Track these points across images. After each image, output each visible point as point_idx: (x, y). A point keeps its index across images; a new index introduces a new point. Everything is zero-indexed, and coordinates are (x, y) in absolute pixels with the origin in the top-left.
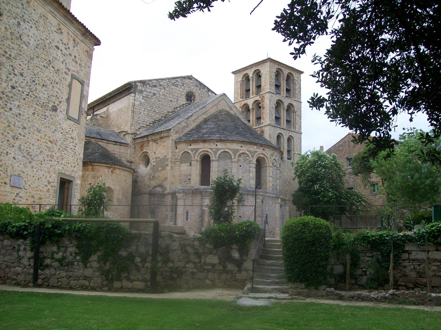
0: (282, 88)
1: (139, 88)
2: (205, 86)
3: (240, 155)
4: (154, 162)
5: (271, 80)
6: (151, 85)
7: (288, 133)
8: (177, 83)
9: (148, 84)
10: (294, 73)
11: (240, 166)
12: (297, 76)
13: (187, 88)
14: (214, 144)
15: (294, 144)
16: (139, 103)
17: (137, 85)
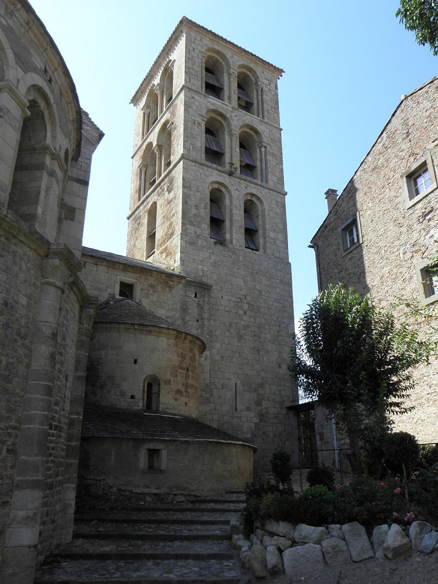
7: (243, 186)
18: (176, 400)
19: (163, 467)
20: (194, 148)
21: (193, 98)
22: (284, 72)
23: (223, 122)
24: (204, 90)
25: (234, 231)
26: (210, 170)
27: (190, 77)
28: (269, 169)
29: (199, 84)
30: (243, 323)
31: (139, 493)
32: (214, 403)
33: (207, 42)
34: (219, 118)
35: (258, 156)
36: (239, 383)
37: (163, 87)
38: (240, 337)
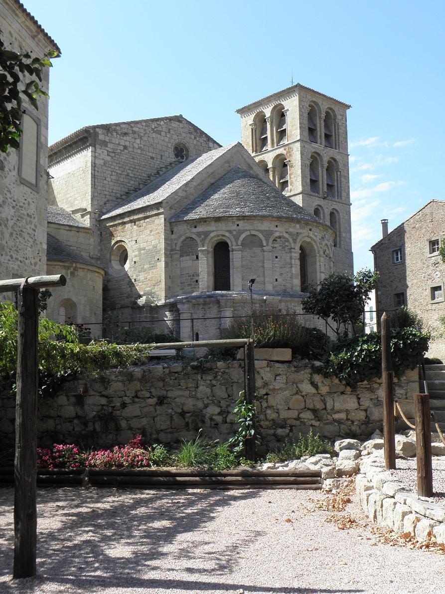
0: (319, 134)
1: (101, 137)
2: (202, 133)
3: (275, 240)
4: (136, 256)
5: (301, 121)
6: (119, 132)
8: (160, 129)
9: (115, 130)
10: (336, 108)
11: (276, 257)
12: (341, 113)
13: (175, 137)
14: (233, 223)
16: (101, 162)
17: (98, 133)
23: (318, 158)
26: (314, 197)
28: (342, 189)
29: (306, 133)
33: (309, 97)
34: (316, 156)
35: (336, 178)
37: (273, 118)
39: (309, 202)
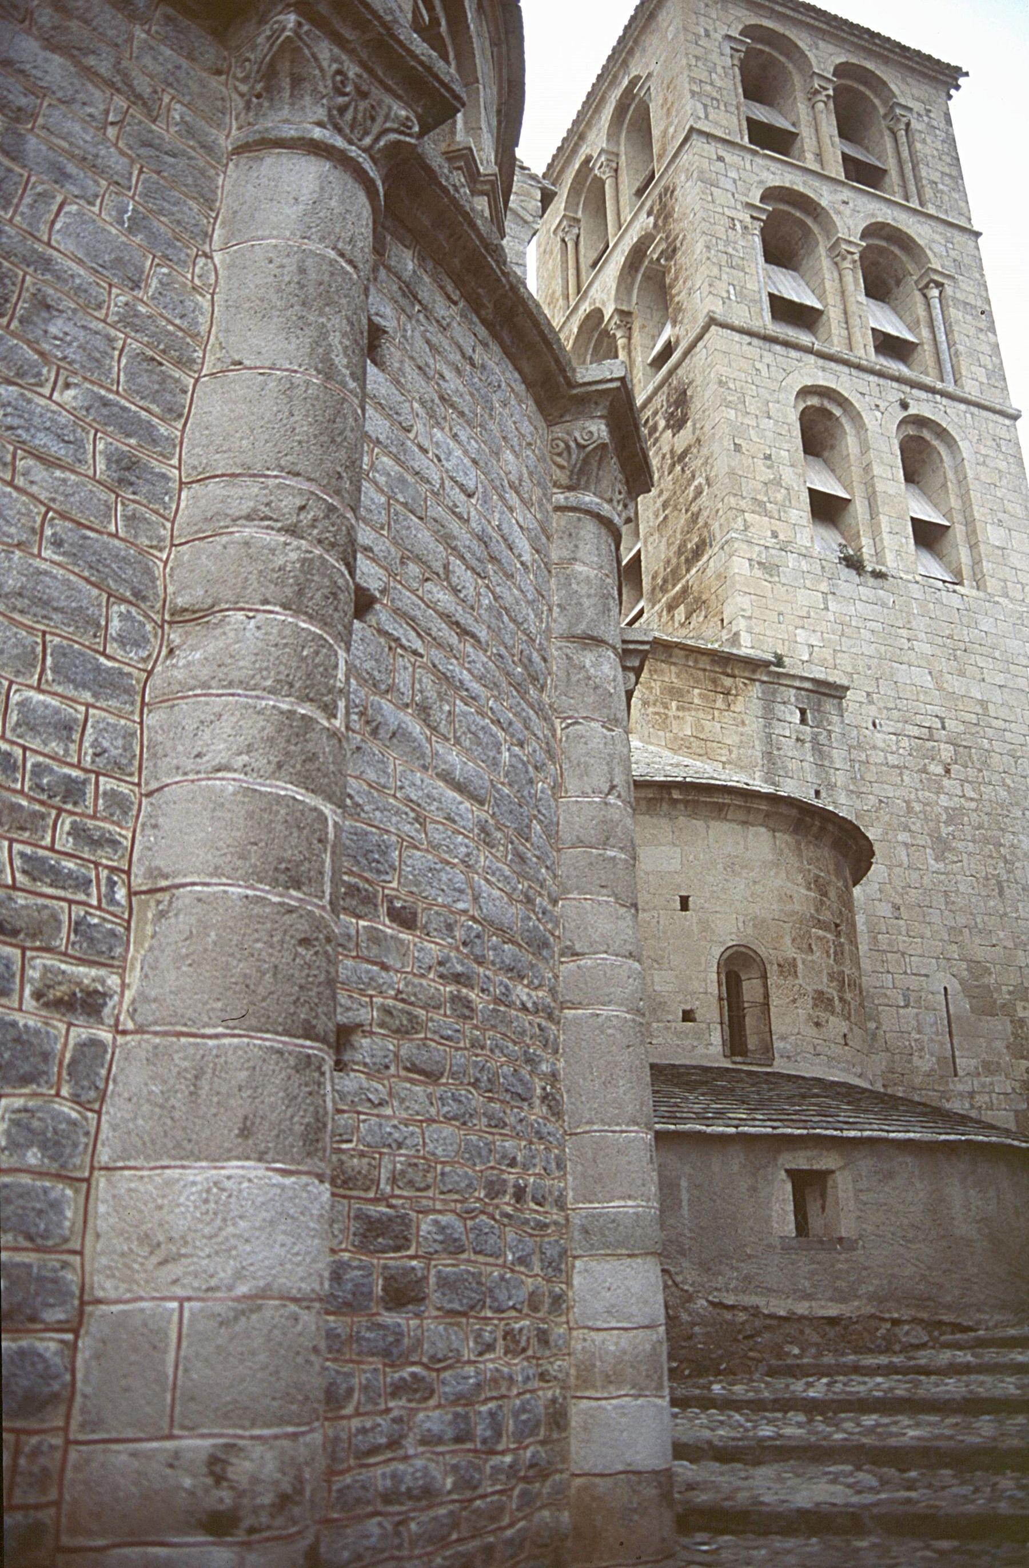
15: (962, 480)
18: (817, 1024)
19: (846, 1228)
20: (741, 295)
21: (720, 159)
22: (967, 74)
23: (809, 222)
24: (746, 138)
25: (885, 528)
27: (705, 106)
28: (961, 348)
30: (944, 800)
31: (781, 1318)
32: (887, 1050)
36: (954, 986)
38: (942, 847)
39: (758, 365)
